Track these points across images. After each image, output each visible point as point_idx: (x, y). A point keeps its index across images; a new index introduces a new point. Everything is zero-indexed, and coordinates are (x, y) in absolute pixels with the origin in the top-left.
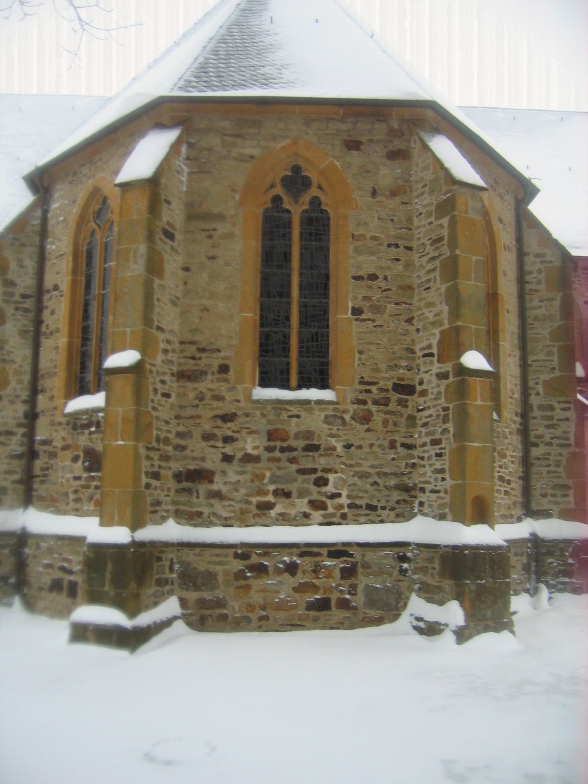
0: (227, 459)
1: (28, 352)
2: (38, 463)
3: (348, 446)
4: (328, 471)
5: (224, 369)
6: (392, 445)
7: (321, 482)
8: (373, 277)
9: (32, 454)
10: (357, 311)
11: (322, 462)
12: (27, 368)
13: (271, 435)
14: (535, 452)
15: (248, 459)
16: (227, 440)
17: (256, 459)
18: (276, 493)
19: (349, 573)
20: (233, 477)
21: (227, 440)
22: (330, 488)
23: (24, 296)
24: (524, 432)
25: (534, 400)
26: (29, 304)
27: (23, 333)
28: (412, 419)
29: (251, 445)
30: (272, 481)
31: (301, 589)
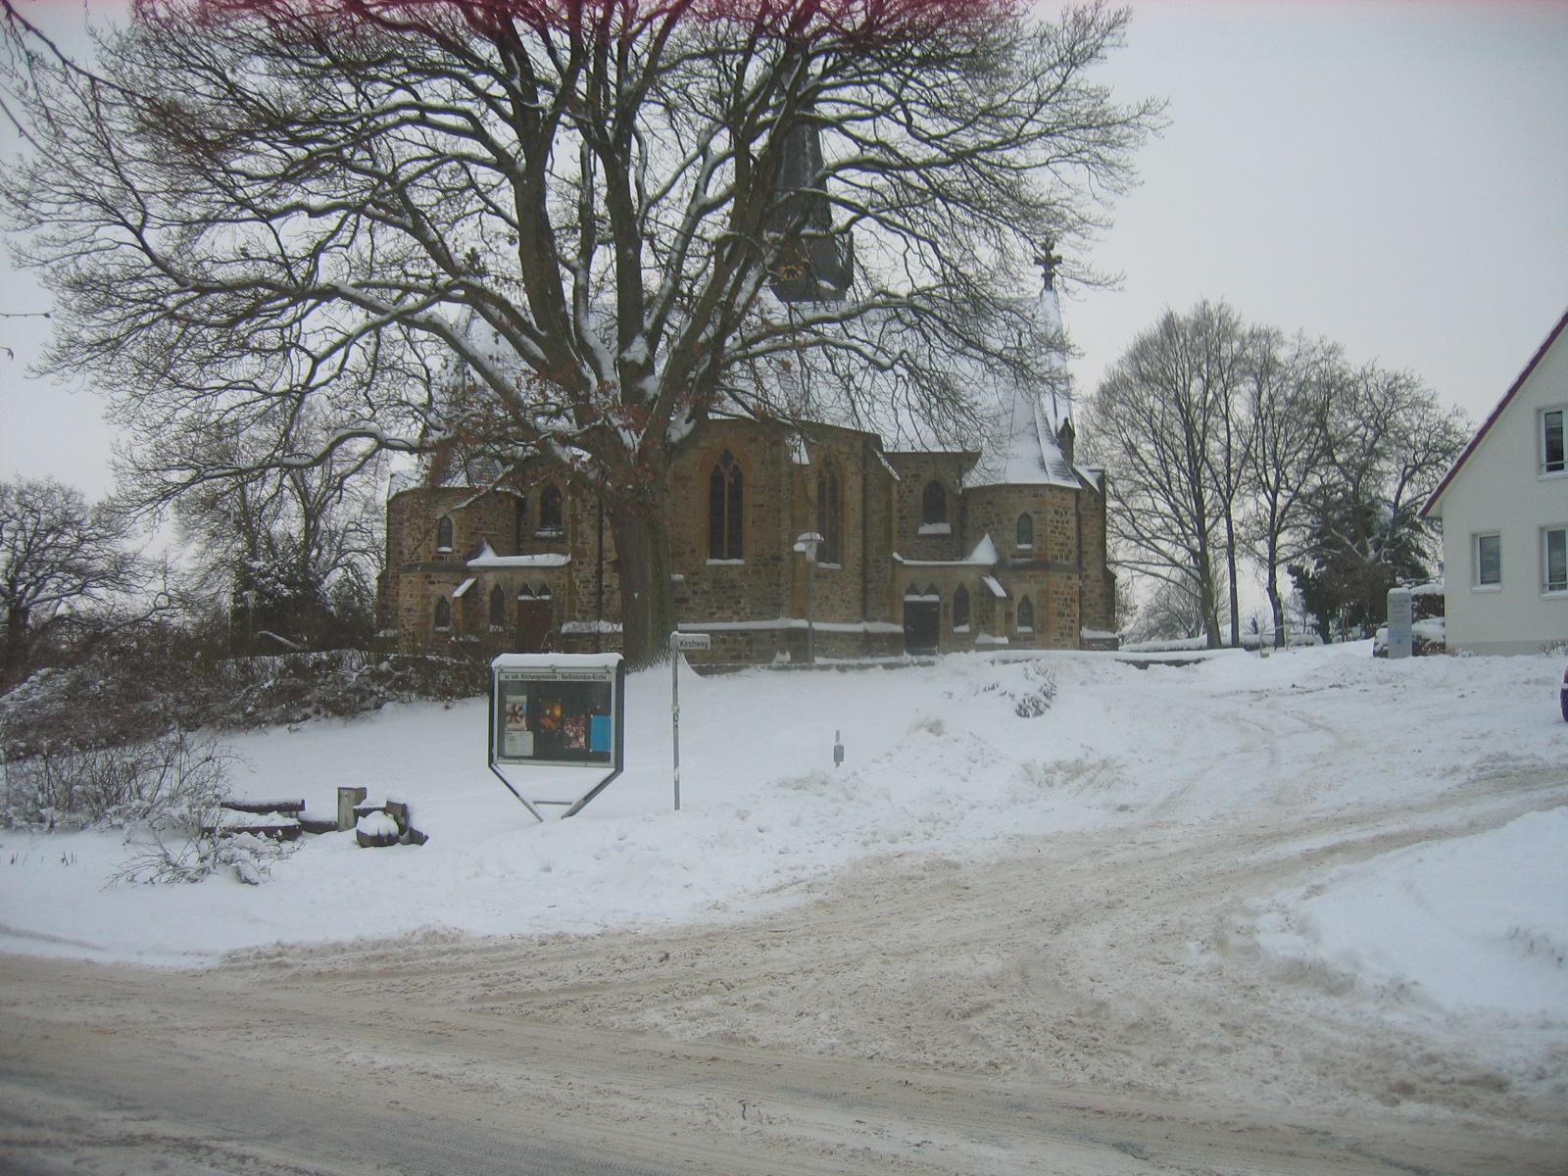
0: (695, 592)
1: (596, 538)
2: (604, 597)
3: (750, 585)
4: (741, 596)
5: (693, 551)
6: (770, 585)
7: (739, 602)
8: (762, 505)
9: (601, 593)
10: (753, 522)
11: (738, 594)
12: (596, 546)
13: (715, 581)
14: (870, 586)
15: (704, 592)
16: (694, 584)
17: (708, 592)
18: (717, 608)
19: (750, 643)
20: (697, 601)
21: (694, 584)
22: (742, 605)
23: (592, 507)
24: (864, 574)
25: (870, 558)
26: (595, 511)
27: (592, 527)
28: (780, 573)
29: (705, 586)
30: (717, 601)
31: (727, 650)
